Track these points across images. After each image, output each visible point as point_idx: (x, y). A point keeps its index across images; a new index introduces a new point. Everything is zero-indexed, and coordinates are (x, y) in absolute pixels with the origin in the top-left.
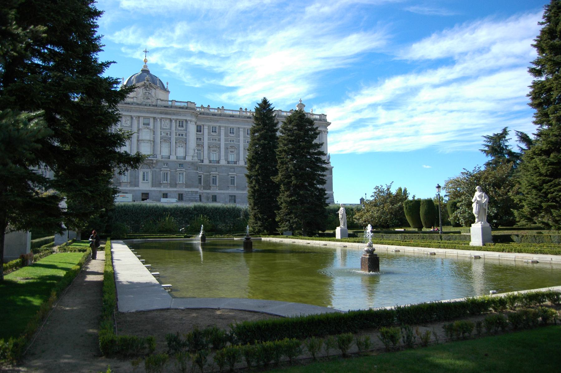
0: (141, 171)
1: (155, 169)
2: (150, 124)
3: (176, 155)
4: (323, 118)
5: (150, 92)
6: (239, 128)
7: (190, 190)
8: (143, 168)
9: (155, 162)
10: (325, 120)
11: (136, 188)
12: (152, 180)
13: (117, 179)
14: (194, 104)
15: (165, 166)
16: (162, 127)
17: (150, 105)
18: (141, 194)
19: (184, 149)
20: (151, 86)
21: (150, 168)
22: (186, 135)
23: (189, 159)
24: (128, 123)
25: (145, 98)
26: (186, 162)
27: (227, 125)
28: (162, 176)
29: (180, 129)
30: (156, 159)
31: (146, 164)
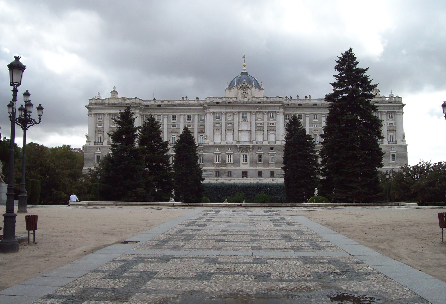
0: (242, 155)
3: (268, 141)
4: (397, 100)
5: (247, 92)
6: (321, 114)
9: (251, 147)
10: (400, 102)
11: (238, 168)
12: (250, 161)
13: (224, 161)
16: (257, 119)
19: (275, 135)
20: (247, 87)
22: (276, 124)
23: (278, 143)
24: (231, 118)
25: (243, 97)
26: (276, 146)
27: (311, 113)
28: (257, 157)
29: (271, 119)
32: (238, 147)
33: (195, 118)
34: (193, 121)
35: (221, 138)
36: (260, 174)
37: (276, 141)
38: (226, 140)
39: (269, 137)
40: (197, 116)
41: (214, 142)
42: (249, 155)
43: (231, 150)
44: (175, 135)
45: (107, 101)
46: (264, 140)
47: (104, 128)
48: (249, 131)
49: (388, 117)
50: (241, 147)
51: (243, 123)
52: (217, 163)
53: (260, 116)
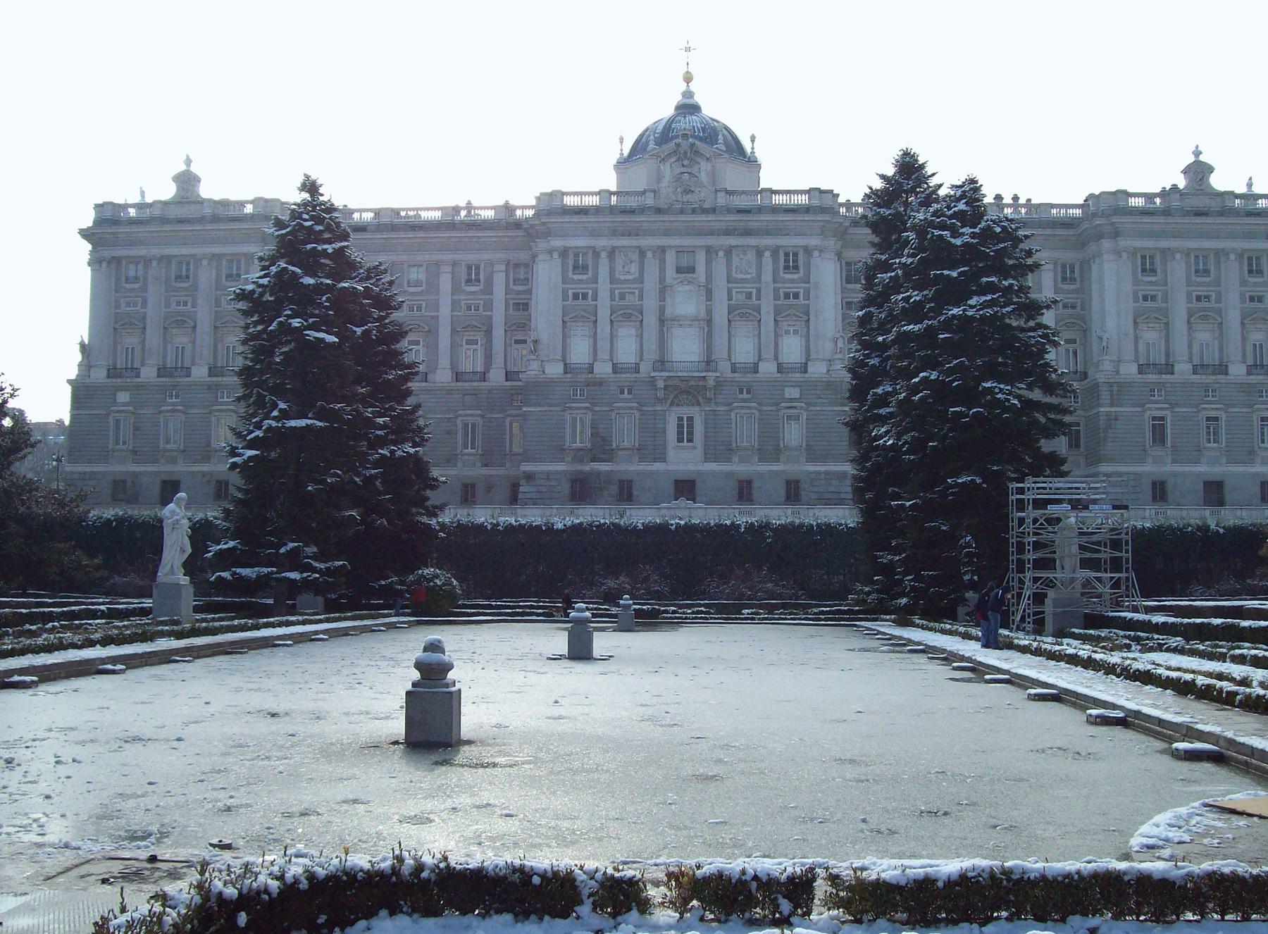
0: (673, 415)
1: (713, 404)
2: (696, 268)
5: (695, 170)
7: (822, 469)
8: (678, 405)
9: (711, 383)
14: (830, 195)
15: (745, 396)
17: (694, 211)
18: (673, 485)
19: (804, 340)
20: (697, 153)
21: (699, 404)
22: (807, 296)
23: (817, 370)
30: (715, 374)
31: (688, 393)
32: (661, 384)
33: (495, 275)
34: (489, 289)
35: (591, 349)
36: (745, 492)
37: (809, 363)
38: (611, 356)
39: (780, 346)
40: (503, 267)
41: (565, 364)
42: (701, 415)
43: (630, 396)
44: (417, 343)
45: (157, 212)
46: (760, 356)
47: (145, 313)
48: (702, 322)
49: (1246, 272)
50: (670, 383)
51: (679, 289)
52: (578, 445)
53: (744, 264)
